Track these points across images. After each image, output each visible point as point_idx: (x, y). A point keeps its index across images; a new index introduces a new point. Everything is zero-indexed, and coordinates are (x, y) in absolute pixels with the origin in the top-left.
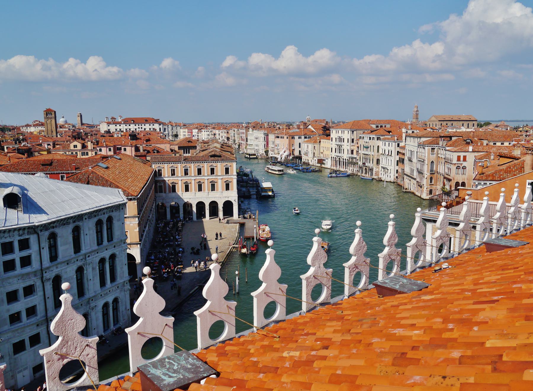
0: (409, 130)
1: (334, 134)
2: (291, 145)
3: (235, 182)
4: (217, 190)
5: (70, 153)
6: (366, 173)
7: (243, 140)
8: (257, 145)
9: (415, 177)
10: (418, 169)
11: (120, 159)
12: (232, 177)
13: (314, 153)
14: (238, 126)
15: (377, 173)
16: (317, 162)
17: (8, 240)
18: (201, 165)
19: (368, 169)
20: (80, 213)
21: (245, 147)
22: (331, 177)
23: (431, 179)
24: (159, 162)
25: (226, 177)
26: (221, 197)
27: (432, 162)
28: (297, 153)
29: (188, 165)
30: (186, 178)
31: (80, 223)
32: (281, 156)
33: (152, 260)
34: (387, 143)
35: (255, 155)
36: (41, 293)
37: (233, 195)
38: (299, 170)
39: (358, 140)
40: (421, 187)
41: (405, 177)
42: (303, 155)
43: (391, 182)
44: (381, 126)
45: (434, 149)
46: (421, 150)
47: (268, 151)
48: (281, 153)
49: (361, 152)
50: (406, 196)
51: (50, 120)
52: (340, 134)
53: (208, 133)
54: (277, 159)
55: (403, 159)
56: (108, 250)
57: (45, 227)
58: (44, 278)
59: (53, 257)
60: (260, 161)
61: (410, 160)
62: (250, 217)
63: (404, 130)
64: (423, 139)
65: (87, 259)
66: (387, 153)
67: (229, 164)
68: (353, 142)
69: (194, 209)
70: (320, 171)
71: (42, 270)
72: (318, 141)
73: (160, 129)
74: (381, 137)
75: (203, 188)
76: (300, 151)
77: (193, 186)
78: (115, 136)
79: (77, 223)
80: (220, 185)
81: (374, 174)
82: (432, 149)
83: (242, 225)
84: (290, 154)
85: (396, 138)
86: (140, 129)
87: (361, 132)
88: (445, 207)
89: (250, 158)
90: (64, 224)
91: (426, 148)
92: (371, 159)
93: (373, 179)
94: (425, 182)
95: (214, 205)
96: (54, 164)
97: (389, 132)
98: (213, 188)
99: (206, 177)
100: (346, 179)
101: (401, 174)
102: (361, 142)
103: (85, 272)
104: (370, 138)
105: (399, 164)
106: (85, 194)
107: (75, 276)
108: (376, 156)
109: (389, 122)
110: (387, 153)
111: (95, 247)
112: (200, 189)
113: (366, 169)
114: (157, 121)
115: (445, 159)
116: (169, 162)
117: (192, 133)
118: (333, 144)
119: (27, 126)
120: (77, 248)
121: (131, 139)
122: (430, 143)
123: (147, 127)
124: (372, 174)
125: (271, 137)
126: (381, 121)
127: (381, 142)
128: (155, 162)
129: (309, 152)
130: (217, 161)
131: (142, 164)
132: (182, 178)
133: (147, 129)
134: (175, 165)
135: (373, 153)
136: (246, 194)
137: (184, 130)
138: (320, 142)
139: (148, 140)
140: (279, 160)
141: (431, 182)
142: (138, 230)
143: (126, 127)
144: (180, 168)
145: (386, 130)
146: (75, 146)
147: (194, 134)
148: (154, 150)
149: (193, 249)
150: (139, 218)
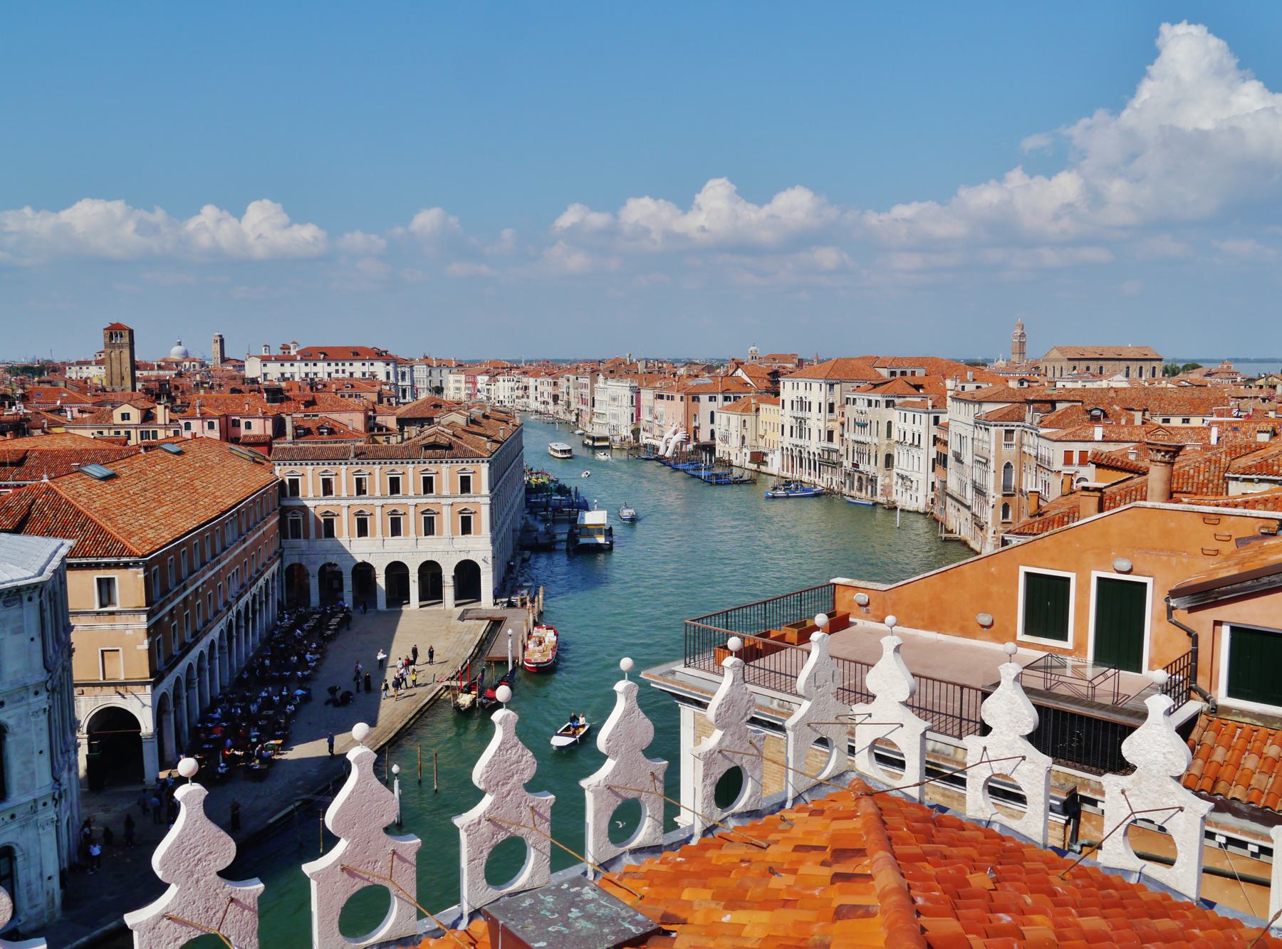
0: (968, 382)
1: (788, 390)
2: (690, 415)
3: (485, 512)
4: (440, 533)
5: (112, 433)
6: (860, 490)
7: (584, 402)
9: (969, 503)
11: (180, 453)
12: (477, 499)
13: (743, 438)
14: (574, 368)
15: (887, 490)
16: (748, 458)
18: (399, 469)
19: (864, 477)
22: (774, 497)
23: (1006, 508)
25: (463, 501)
26: (449, 550)
28: (704, 437)
29: (366, 469)
30: (359, 503)
33: (212, 720)
34: (910, 415)
35: (606, 439)
37: (480, 548)
38: (699, 477)
41: (949, 500)
42: (718, 441)
43: (917, 512)
44: (903, 373)
45: (1012, 431)
46: (981, 434)
47: (638, 430)
50: (951, 546)
51: (117, 351)
52: (801, 392)
53: (512, 384)
55: (946, 456)
60: (617, 455)
61: (958, 459)
62: (524, 604)
63: (949, 384)
64: (988, 408)
66: (909, 439)
67: (470, 468)
68: (831, 410)
69: (381, 581)
70: (752, 482)
73: (388, 374)
74: (897, 401)
75: (409, 523)
76: (712, 433)
77: (378, 523)
80: (447, 520)
81: (879, 492)
84: (688, 440)
85: (930, 403)
86: (340, 375)
87: (850, 386)
88: (738, 654)
91: (993, 429)
92: (873, 454)
93: (875, 504)
94: (990, 516)
96: (28, 463)
97: (918, 387)
98: (429, 528)
99: (411, 502)
100: (812, 501)
101: (941, 492)
105: (938, 467)
108: (883, 447)
109: (922, 362)
110: (909, 439)
112: (396, 530)
113: (860, 478)
114: (380, 355)
115: (1037, 457)
116: (317, 458)
117: (475, 383)
118: (786, 416)
119: (80, 364)
121: (268, 400)
122: (1001, 418)
123: (358, 369)
124: (874, 493)
125: (647, 396)
126: (902, 359)
129: (730, 433)
130: (439, 460)
132: (351, 502)
133: (358, 375)
134: (332, 469)
135: (876, 440)
136: (542, 540)
138: (758, 410)
140: (661, 452)
141: (1005, 515)
142: (146, 646)
143: (307, 369)
144: (344, 476)
145: (911, 383)
147: (479, 386)
148: (322, 427)
149: (332, 690)
150: (150, 615)
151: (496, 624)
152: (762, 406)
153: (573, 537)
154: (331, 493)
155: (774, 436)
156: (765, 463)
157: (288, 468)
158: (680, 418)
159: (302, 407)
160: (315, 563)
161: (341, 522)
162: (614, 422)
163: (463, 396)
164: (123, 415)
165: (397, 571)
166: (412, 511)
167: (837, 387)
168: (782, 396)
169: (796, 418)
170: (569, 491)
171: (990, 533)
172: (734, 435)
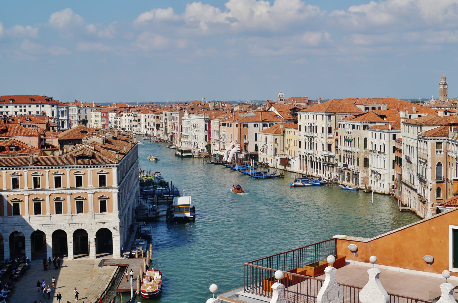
0: (413, 113)
1: (303, 120)
2: (242, 136)
3: (115, 198)
4: (87, 212)
6: (349, 181)
7: (176, 128)
8: (195, 137)
9: (416, 187)
10: (419, 175)
13: (276, 149)
14: (170, 107)
15: (365, 181)
16: (279, 162)
18: (61, 171)
19: (351, 173)
21: (178, 139)
22: (295, 186)
23: (439, 190)
25: (101, 191)
27: (439, 164)
28: (251, 149)
29: (40, 172)
30: (35, 193)
32: (228, 153)
34: (378, 134)
35: (189, 151)
37: (112, 221)
38: (248, 174)
39: (336, 129)
40: (424, 203)
41: (403, 186)
42: (259, 152)
43: (384, 194)
44: (373, 108)
45: (441, 143)
46: (422, 145)
48: (228, 149)
49: (342, 147)
52: (311, 121)
53: (130, 118)
54: (222, 158)
55: (401, 159)
60: (196, 160)
61: (409, 160)
62: (140, 256)
63: (402, 114)
64: (426, 129)
66: (378, 149)
67: (105, 170)
68: (330, 132)
69: (49, 242)
70: (282, 177)
72: (282, 131)
74: (370, 125)
76: (256, 147)
77: (48, 205)
80: (91, 203)
81: (360, 182)
82: (438, 143)
83: (122, 268)
84: (241, 151)
85: (390, 126)
86: (23, 113)
89: (182, 157)
91: (429, 142)
93: (358, 189)
94: (429, 195)
95: (81, 235)
98: (80, 209)
99: (68, 192)
100: (319, 188)
101: (398, 181)
102: (341, 132)
104: (353, 127)
108: (362, 154)
109: (384, 101)
112: (59, 210)
113: (348, 174)
114: (48, 101)
115: (456, 159)
117: (107, 117)
118: (302, 136)
122: (434, 135)
123: (34, 109)
124: (357, 182)
125: (215, 125)
126: (373, 100)
127: (370, 132)
130: (86, 165)
133: (34, 113)
134: (19, 172)
135: (357, 150)
136: (151, 215)
137: (96, 114)
138: (284, 132)
140: (224, 159)
141: (438, 195)
144: (25, 177)
145: (378, 114)
147: (110, 119)
148: (12, 145)
151: (122, 268)
152: (287, 130)
153: (170, 213)
154: (18, 187)
155: (294, 148)
156: (289, 165)
158: (236, 138)
160: (7, 232)
162: (194, 141)
163: (100, 125)
165: (60, 236)
166: (69, 198)
167: (333, 117)
168: (299, 124)
169: (308, 137)
170: (167, 184)
171: (429, 206)
172: (270, 148)
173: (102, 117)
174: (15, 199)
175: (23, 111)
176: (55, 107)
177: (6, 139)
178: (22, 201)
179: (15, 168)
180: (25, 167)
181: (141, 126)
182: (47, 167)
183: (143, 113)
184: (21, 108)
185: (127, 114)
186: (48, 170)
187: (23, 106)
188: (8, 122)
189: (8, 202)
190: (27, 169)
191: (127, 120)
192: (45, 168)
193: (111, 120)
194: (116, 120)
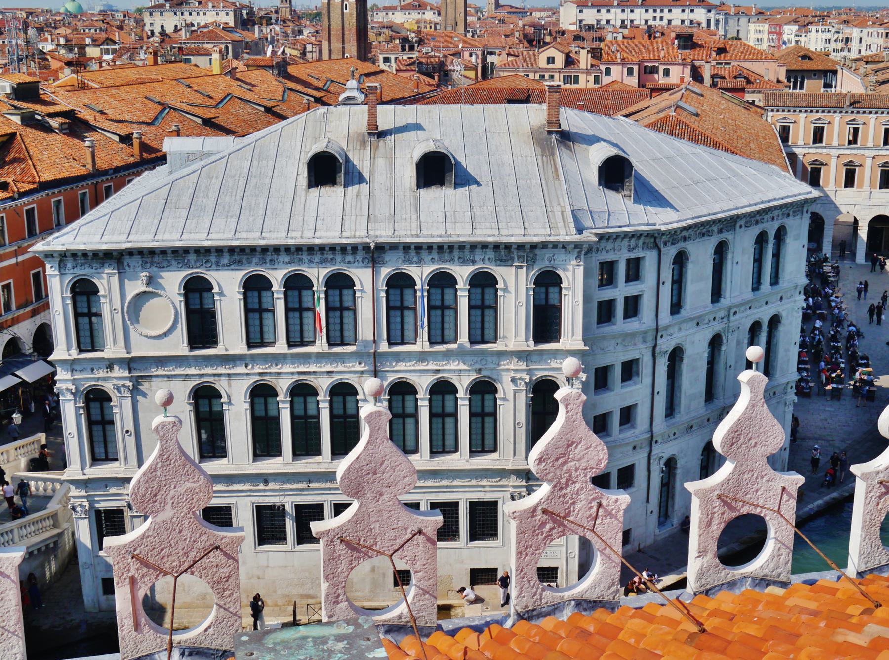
5: (537, 77)
17: (610, 257)
20: (734, 212)
24: (785, 107)
29: (861, 118)
30: (850, 153)
31: (727, 236)
36: (648, 380)
53: (827, 35)
56: (770, 305)
57: (674, 236)
58: (658, 349)
59: (676, 307)
65: (732, 318)
69: (863, 233)
71: (657, 330)
73: (709, 21)
78: (609, 37)
79: (725, 235)
90: (703, 235)
103: (724, 348)
106: (733, 170)
107: (706, 355)
111: (748, 294)
116: (810, 107)
117: (780, 34)
119: (387, 9)
120: (717, 293)
121: (679, 47)
128: (776, 108)
131: (744, 110)
133: (676, 22)
137: (760, 26)
139: (721, 51)
143: (624, 16)
144: (837, 126)
146: (551, 60)
147: (785, 37)
154: (821, 141)
157: (781, 115)
159: (714, 54)
161: (829, 171)
163: (764, 46)
164: (548, 58)
173: (770, 32)
174: (816, 160)
175: (658, 19)
176: (713, 12)
177: (726, 64)
178: (826, 164)
179: (820, 110)
180: (838, 110)
181: (849, 50)
182: (874, 111)
183: (856, 26)
184: (655, 15)
185: (820, 28)
186: (875, 116)
187: (658, 11)
188: (655, 37)
189: (803, 165)
190: (841, 112)
191: (819, 40)
192: (870, 113)
193: (788, 40)
194: (797, 38)
